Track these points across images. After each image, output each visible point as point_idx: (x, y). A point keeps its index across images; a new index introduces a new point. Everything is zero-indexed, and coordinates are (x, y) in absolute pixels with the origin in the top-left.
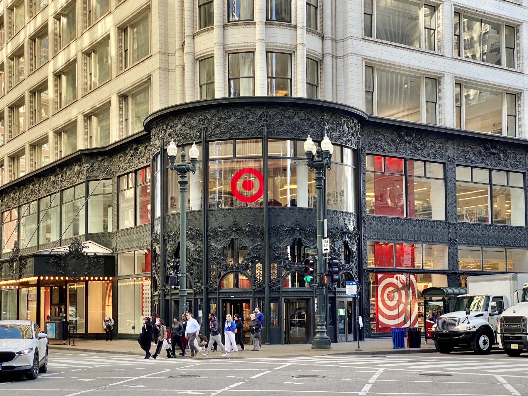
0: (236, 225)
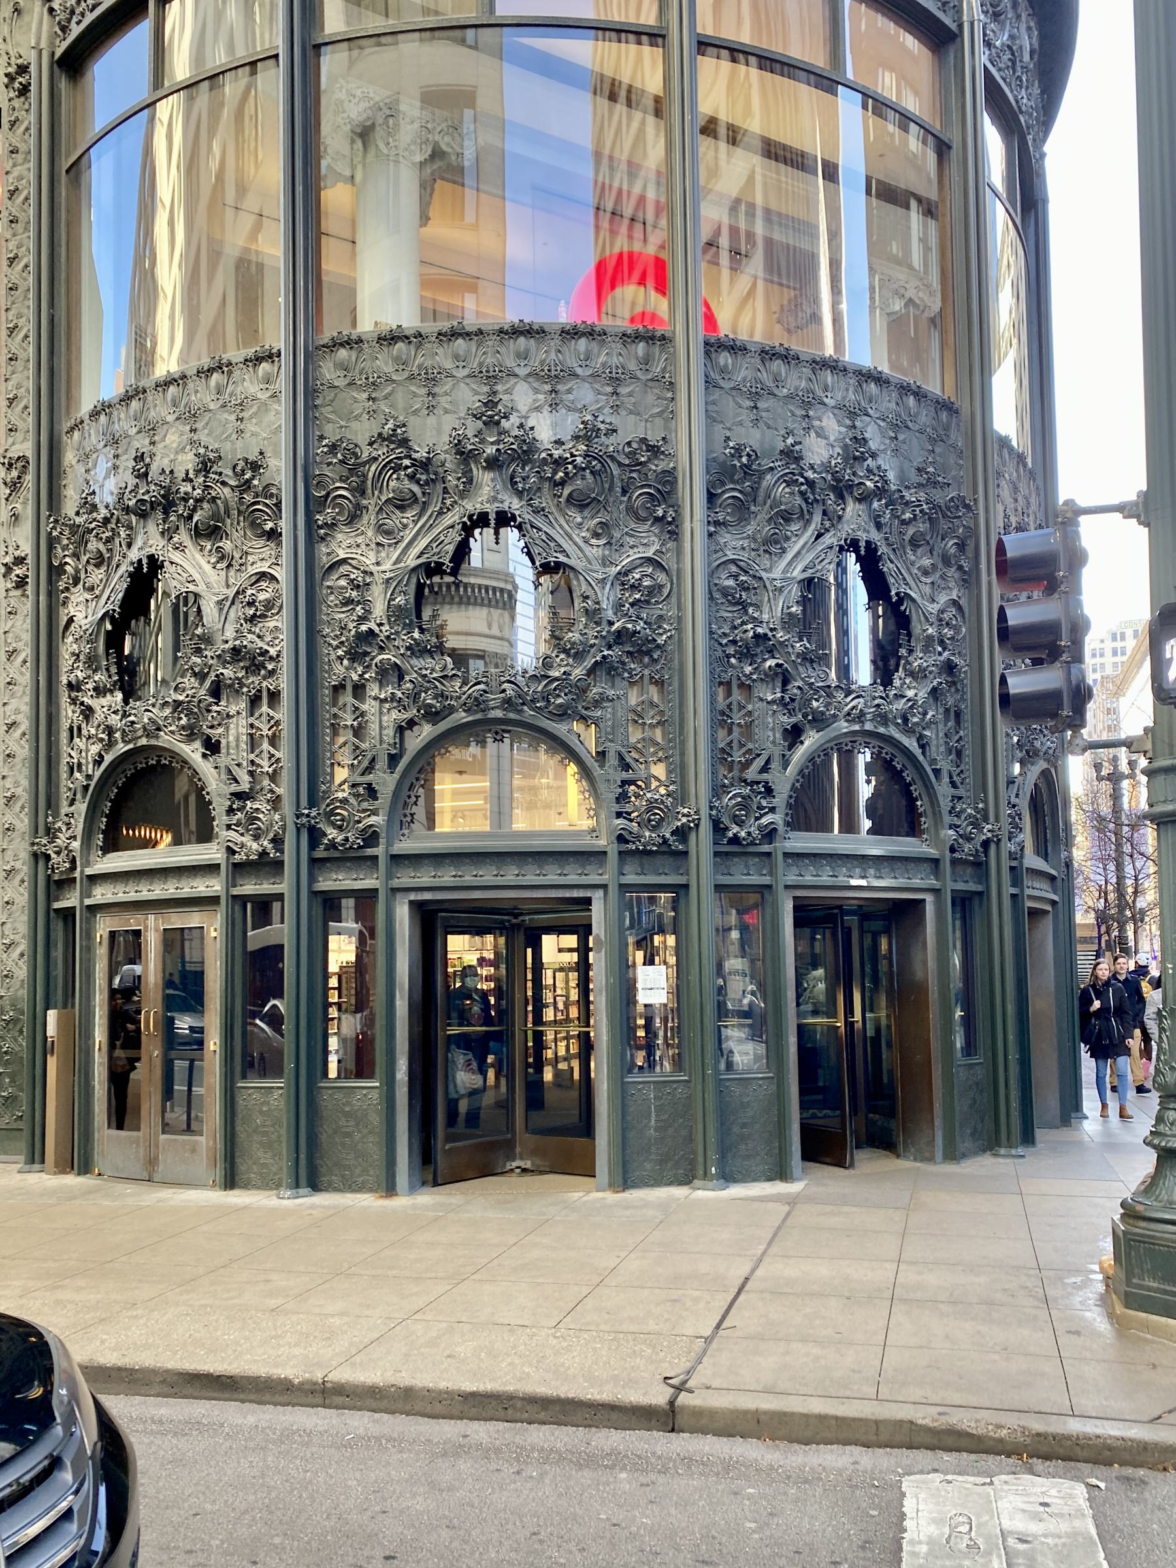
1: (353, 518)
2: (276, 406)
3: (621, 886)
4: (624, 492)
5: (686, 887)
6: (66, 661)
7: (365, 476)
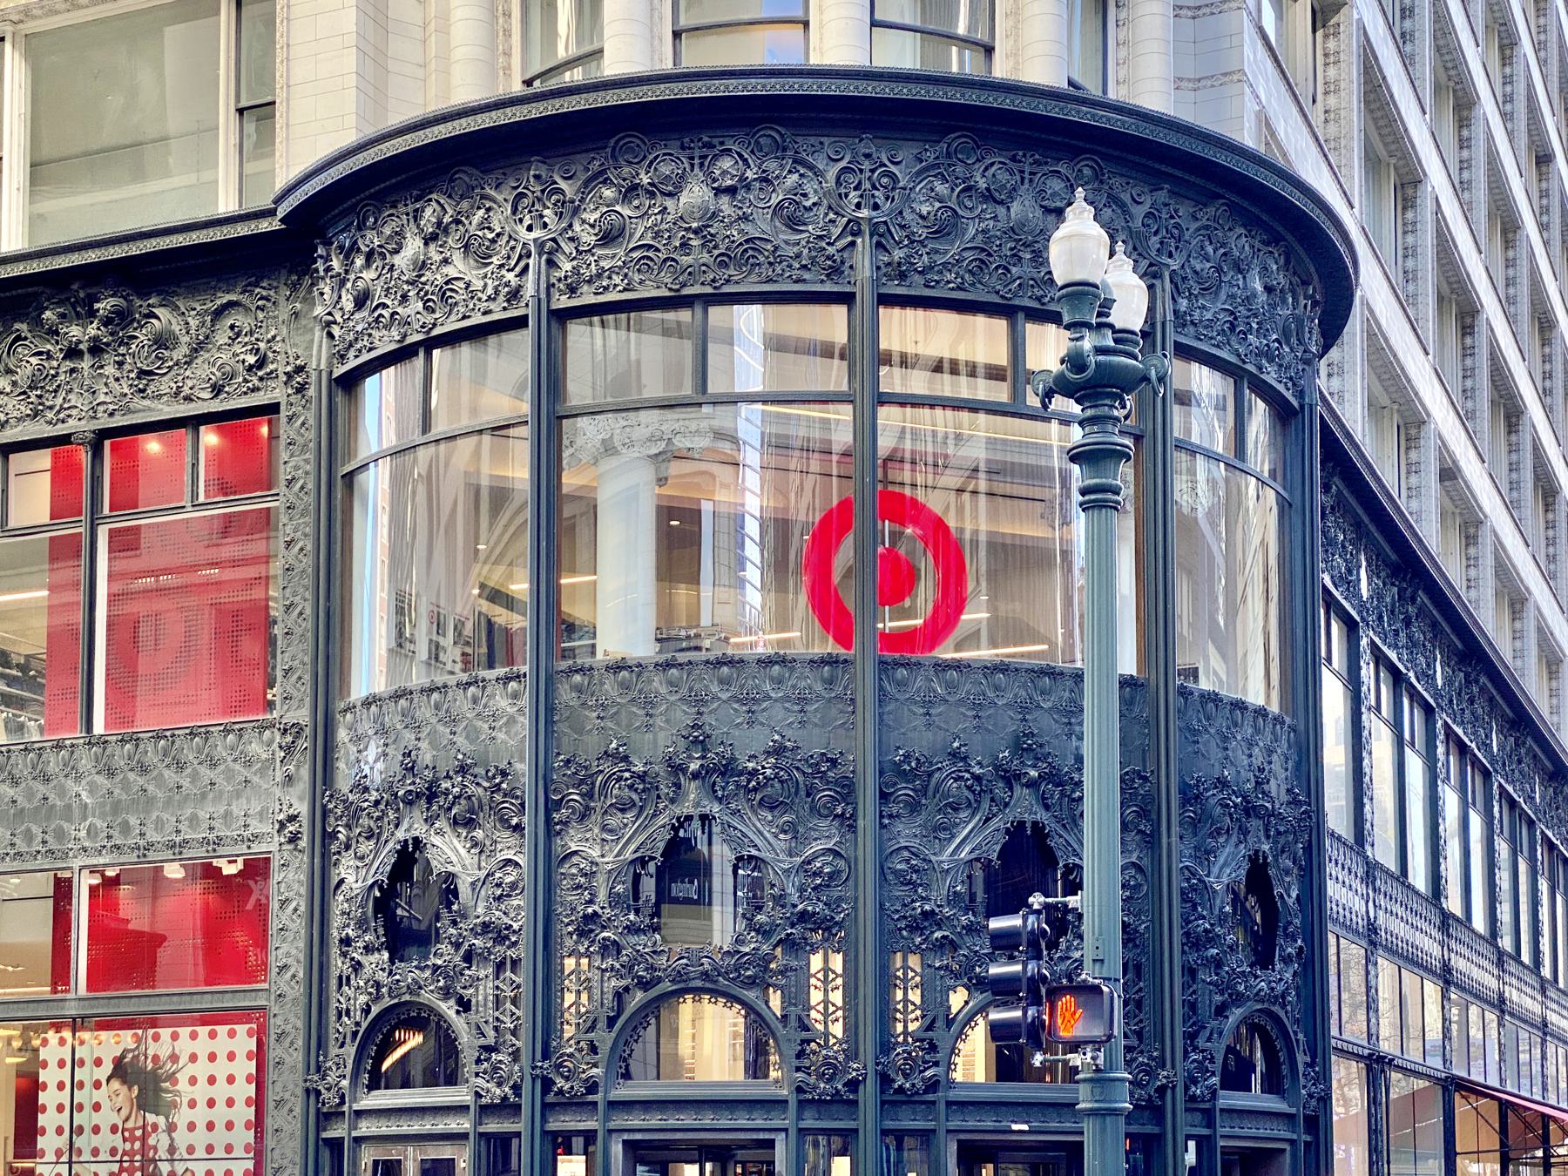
0: (702, 744)
1: (583, 817)
2: (521, 719)
3: (800, 1130)
4: (808, 795)
5: (856, 1131)
6: (337, 921)
7: (593, 784)
